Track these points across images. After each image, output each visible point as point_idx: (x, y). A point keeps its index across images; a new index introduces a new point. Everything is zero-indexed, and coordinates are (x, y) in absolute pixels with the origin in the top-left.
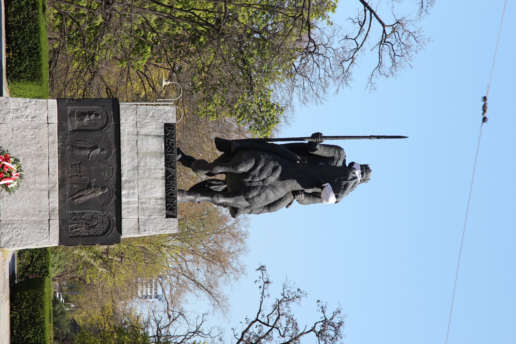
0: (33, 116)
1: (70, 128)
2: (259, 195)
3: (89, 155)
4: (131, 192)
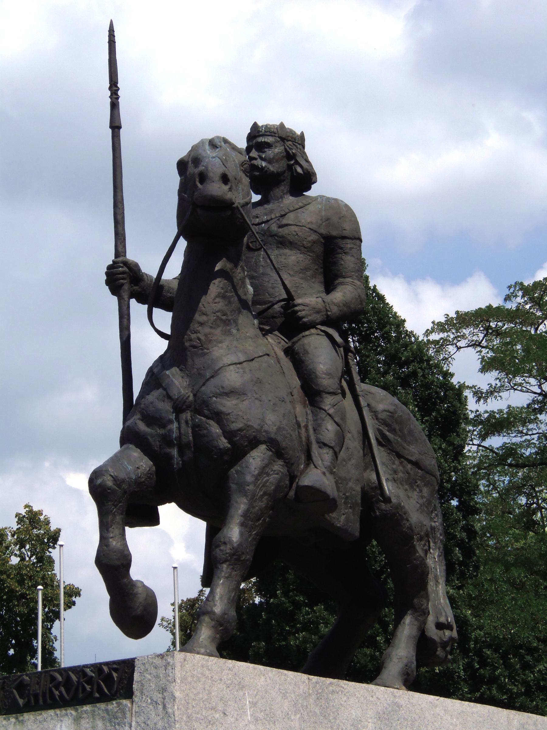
2: (218, 417)
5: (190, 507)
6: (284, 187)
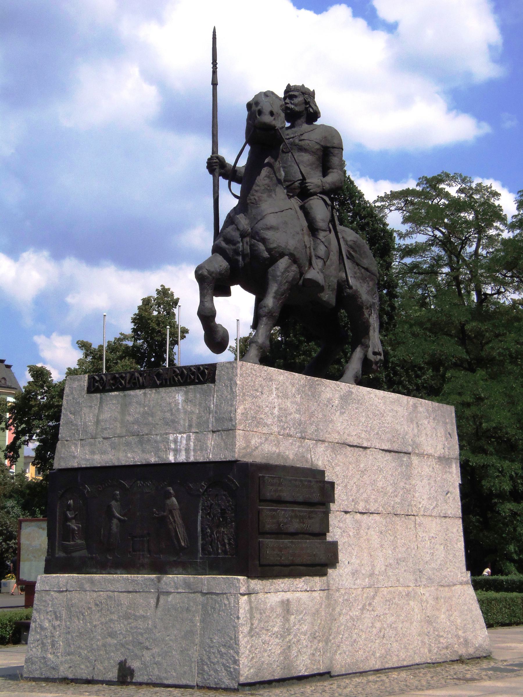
0: (53, 616)
1: (84, 553)
2: (264, 241)
3: (119, 519)
4: (173, 446)
5: (247, 287)
6: (303, 119)
